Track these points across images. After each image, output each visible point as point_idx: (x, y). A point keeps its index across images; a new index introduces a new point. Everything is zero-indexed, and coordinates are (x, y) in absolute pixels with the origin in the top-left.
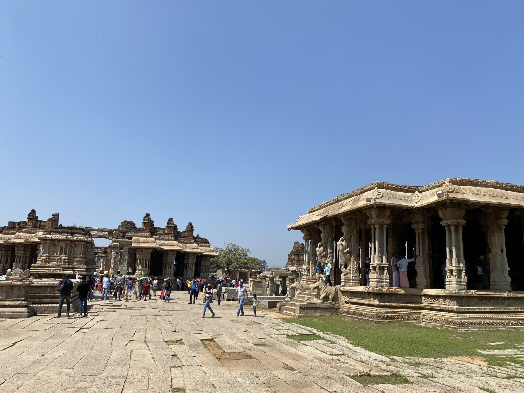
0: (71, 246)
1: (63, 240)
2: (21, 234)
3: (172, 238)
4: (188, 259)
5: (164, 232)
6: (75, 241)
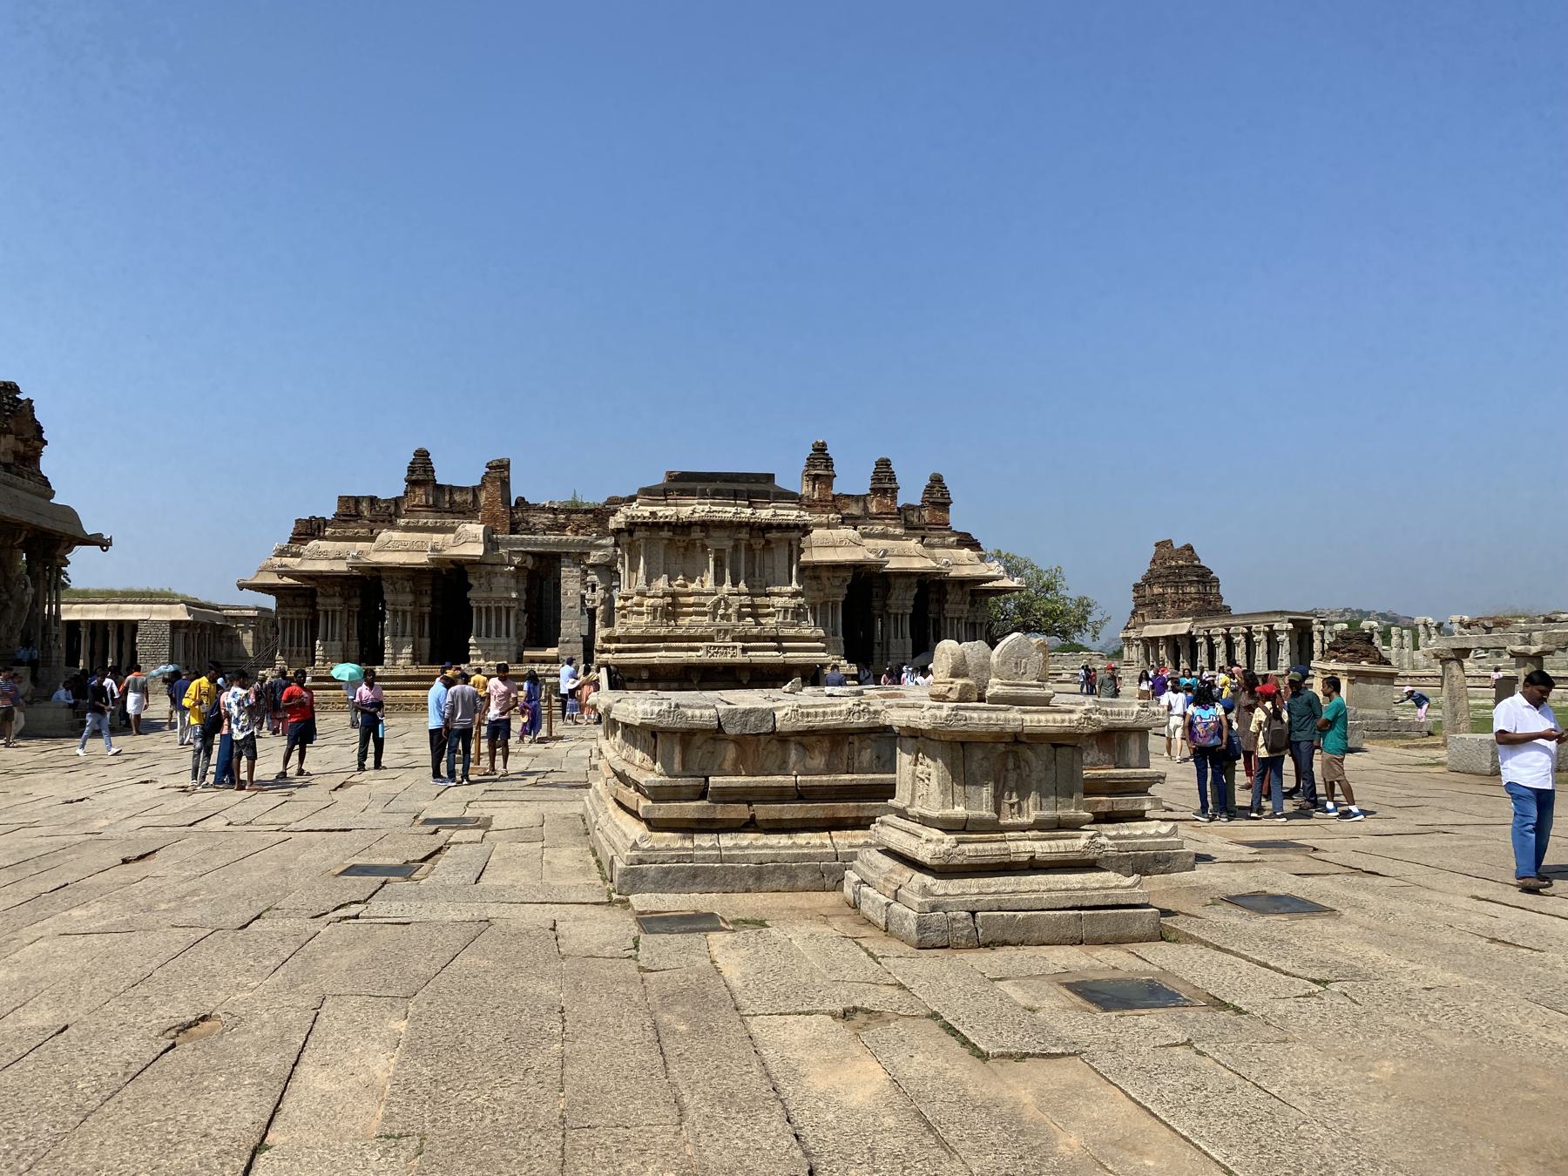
0: (749, 548)
1: (722, 525)
2: (397, 535)
3: (899, 531)
4: (941, 601)
5: (866, 508)
6: (768, 527)
